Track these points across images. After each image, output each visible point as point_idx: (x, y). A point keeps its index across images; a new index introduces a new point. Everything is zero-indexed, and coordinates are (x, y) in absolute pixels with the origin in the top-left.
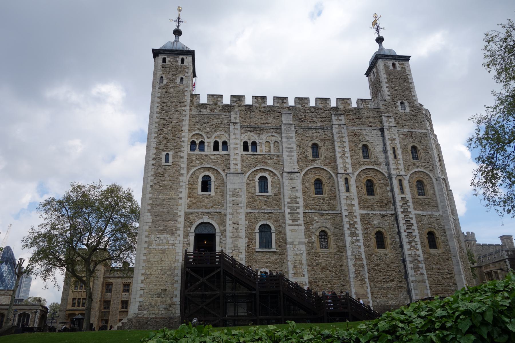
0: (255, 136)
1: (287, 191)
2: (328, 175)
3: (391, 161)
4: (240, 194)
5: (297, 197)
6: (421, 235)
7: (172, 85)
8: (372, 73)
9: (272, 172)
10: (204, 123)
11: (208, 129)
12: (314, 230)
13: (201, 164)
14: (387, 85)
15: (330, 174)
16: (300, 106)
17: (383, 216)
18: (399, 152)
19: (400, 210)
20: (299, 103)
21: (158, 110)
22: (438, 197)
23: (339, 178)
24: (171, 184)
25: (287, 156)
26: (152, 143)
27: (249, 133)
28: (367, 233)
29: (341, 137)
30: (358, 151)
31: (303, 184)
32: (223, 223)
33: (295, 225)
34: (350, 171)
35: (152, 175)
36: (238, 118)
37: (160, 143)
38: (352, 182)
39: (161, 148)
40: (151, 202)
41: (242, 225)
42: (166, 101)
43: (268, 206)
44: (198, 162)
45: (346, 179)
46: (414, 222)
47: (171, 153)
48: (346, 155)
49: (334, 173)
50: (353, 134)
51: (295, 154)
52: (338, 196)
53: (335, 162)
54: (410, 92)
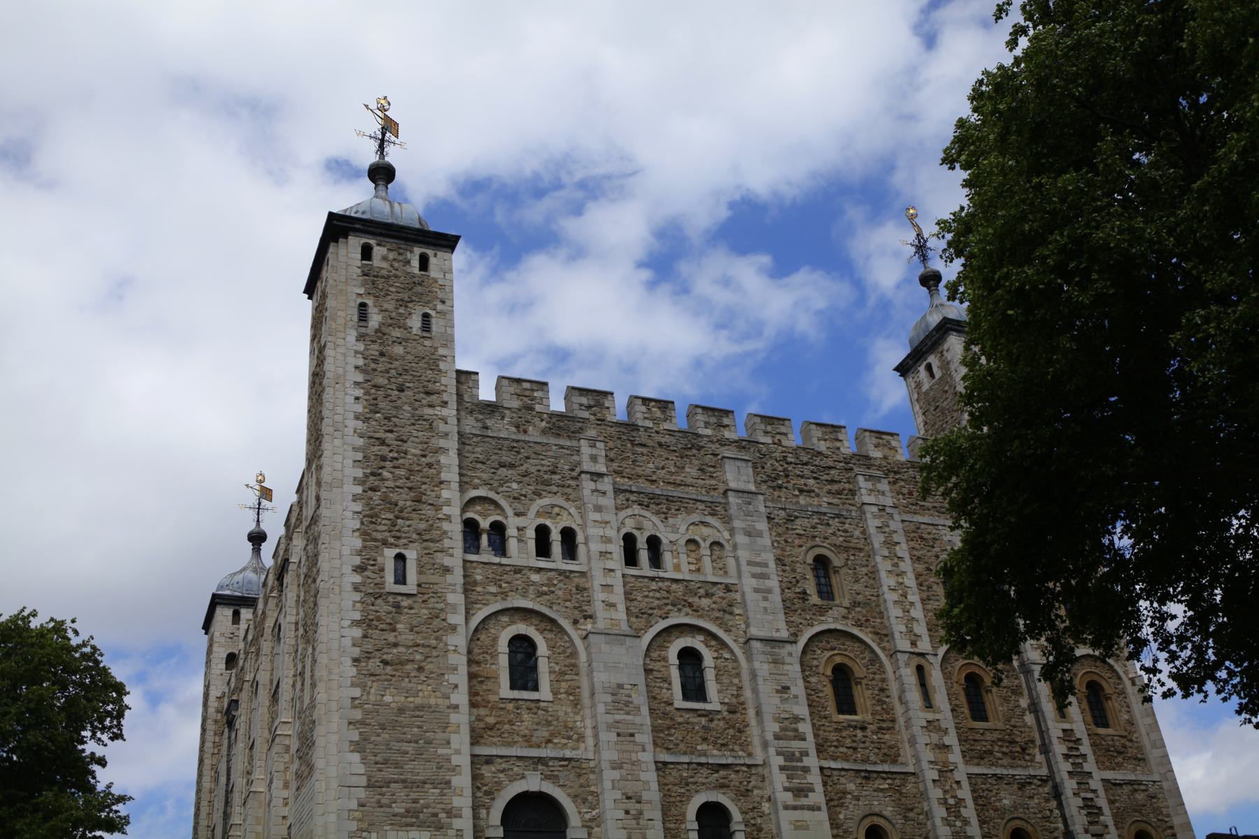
0: (655, 519)
1: (771, 702)
2: (867, 655)
5: (797, 719)
7: (397, 333)
8: (922, 369)
9: (714, 636)
10: (502, 465)
11: (515, 486)
13: (504, 595)
15: (873, 651)
16: (768, 440)
17: (1022, 786)
19: (1064, 767)
20: (766, 433)
21: (359, 408)
22: (1143, 731)
23: (901, 663)
24: (418, 657)
25: (756, 590)
26: (350, 514)
27: (636, 509)
29: (890, 544)
30: (935, 587)
31: (805, 679)
32: (587, 798)
33: (802, 808)
34: (924, 645)
35: (356, 623)
36: (602, 460)
37: (370, 517)
38: (936, 677)
39: (379, 536)
40: (358, 715)
41: (649, 802)
42: (381, 381)
43: (715, 744)
44: (493, 589)
45: (920, 669)
46: (1102, 802)
47: (411, 555)
48: (911, 598)
49: (883, 649)
51: (774, 583)
52: (901, 721)
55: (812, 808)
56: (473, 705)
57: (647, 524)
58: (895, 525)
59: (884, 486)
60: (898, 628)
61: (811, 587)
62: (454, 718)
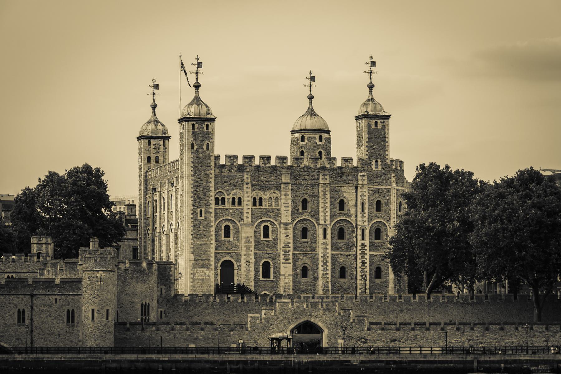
0: (262, 193)
1: (282, 239)
3: (359, 214)
4: (251, 240)
5: (289, 243)
6: (370, 270)
7: (200, 151)
10: (225, 182)
12: (299, 266)
14: (367, 144)
16: (296, 165)
17: (347, 256)
18: (366, 206)
19: (359, 252)
20: (296, 163)
21: (192, 173)
27: (257, 191)
28: (334, 268)
29: (325, 195)
31: (294, 231)
32: (239, 261)
35: (192, 226)
36: (249, 178)
37: (195, 201)
38: (329, 231)
40: (192, 246)
42: (197, 165)
47: (203, 210)
50: (334, 191)
51: (290, 209)
53: (318, 214)
54: (385, 151)
55: (289, 263)
56: (216, 241)
57: (259, 195)
58: (328, 189)
59: (327, 177)
60: (321, 218)
61: (300, 208)
62: (211, 246)
